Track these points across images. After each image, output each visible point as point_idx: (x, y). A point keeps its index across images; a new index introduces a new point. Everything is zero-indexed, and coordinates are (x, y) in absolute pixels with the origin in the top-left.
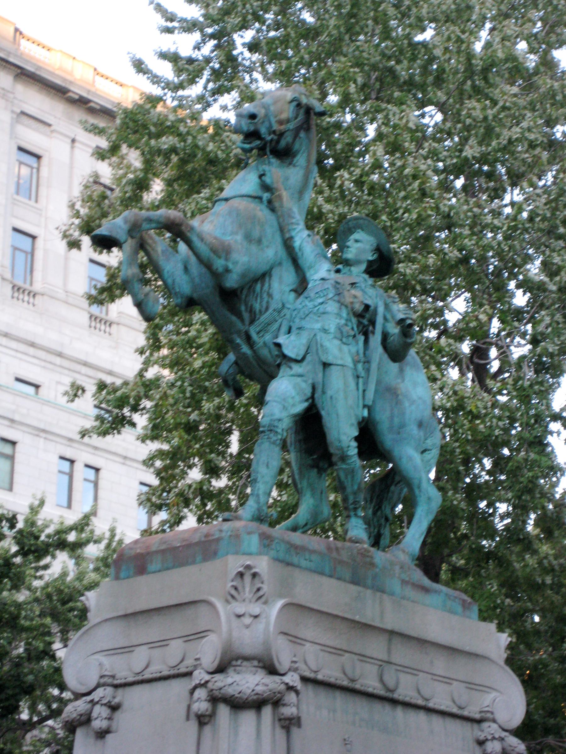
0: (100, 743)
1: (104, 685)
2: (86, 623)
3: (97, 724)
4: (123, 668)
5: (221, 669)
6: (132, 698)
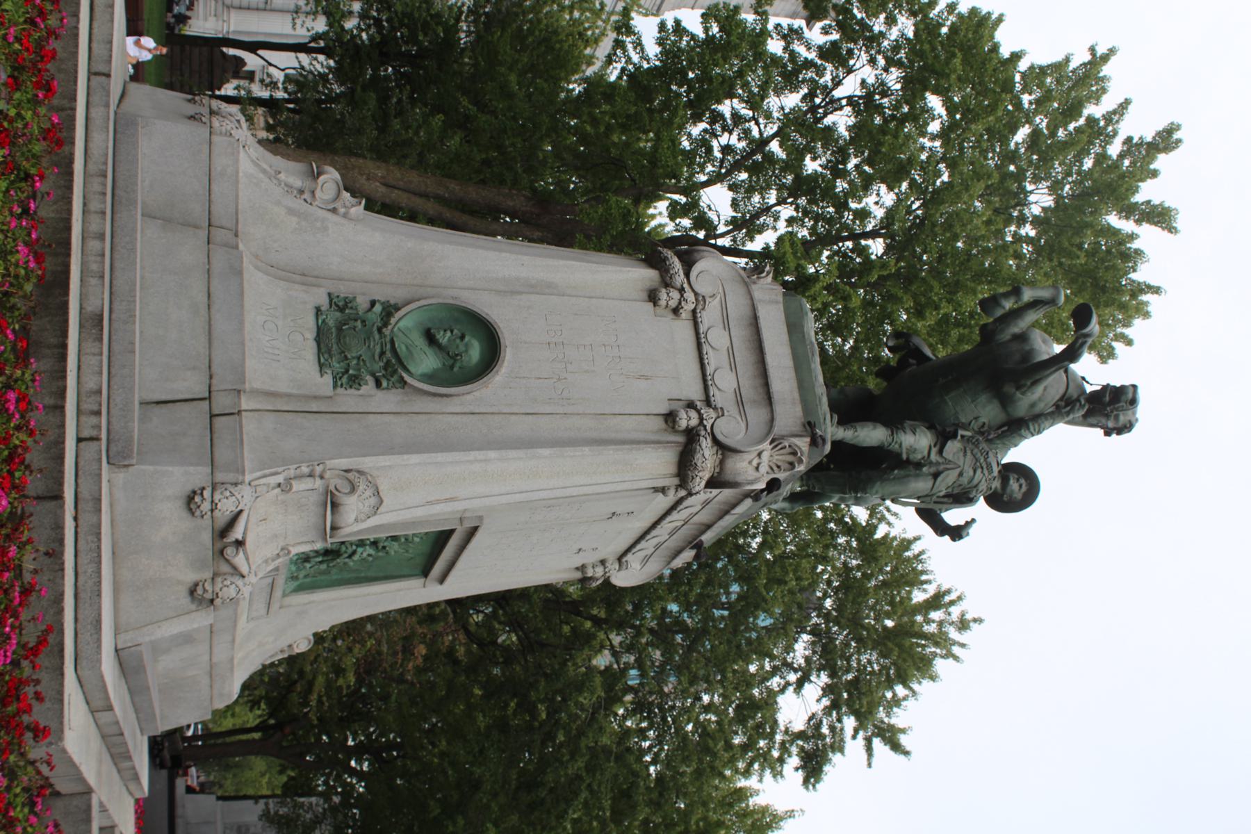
0: (645, 295)
1: (697, 300)
2: (836, 417)
3: (663, 295)
4: (710, 317)
5: (716, 441)
6: (683, 327)
